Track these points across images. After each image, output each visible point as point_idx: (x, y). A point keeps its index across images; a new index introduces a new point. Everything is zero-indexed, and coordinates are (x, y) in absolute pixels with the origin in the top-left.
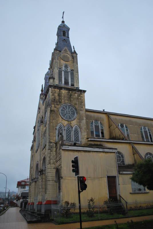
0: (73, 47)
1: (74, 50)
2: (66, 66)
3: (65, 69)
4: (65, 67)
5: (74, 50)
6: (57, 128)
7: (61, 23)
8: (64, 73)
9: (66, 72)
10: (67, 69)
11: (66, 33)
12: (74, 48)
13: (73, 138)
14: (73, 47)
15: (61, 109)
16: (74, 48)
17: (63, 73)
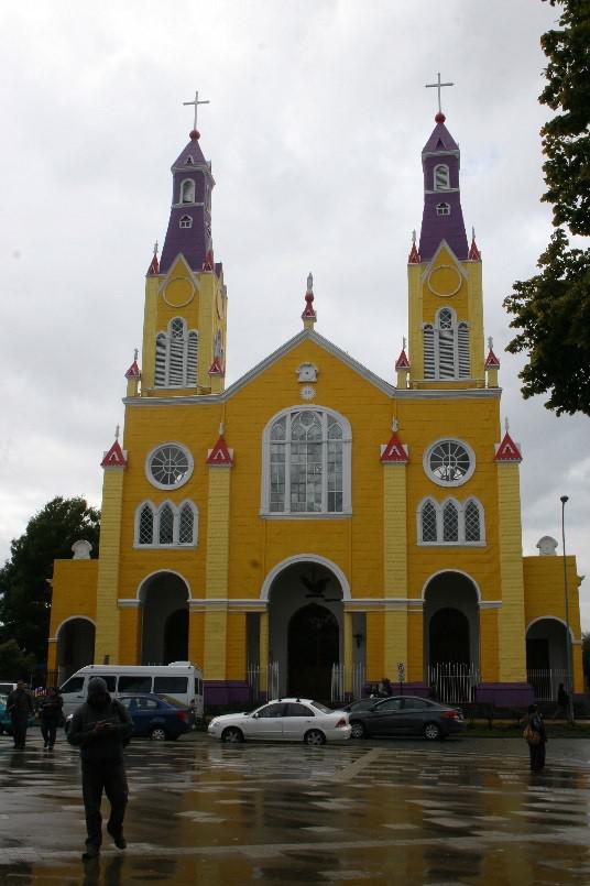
4: (441, 316)
6: (420, 508)
13: (461, 534)
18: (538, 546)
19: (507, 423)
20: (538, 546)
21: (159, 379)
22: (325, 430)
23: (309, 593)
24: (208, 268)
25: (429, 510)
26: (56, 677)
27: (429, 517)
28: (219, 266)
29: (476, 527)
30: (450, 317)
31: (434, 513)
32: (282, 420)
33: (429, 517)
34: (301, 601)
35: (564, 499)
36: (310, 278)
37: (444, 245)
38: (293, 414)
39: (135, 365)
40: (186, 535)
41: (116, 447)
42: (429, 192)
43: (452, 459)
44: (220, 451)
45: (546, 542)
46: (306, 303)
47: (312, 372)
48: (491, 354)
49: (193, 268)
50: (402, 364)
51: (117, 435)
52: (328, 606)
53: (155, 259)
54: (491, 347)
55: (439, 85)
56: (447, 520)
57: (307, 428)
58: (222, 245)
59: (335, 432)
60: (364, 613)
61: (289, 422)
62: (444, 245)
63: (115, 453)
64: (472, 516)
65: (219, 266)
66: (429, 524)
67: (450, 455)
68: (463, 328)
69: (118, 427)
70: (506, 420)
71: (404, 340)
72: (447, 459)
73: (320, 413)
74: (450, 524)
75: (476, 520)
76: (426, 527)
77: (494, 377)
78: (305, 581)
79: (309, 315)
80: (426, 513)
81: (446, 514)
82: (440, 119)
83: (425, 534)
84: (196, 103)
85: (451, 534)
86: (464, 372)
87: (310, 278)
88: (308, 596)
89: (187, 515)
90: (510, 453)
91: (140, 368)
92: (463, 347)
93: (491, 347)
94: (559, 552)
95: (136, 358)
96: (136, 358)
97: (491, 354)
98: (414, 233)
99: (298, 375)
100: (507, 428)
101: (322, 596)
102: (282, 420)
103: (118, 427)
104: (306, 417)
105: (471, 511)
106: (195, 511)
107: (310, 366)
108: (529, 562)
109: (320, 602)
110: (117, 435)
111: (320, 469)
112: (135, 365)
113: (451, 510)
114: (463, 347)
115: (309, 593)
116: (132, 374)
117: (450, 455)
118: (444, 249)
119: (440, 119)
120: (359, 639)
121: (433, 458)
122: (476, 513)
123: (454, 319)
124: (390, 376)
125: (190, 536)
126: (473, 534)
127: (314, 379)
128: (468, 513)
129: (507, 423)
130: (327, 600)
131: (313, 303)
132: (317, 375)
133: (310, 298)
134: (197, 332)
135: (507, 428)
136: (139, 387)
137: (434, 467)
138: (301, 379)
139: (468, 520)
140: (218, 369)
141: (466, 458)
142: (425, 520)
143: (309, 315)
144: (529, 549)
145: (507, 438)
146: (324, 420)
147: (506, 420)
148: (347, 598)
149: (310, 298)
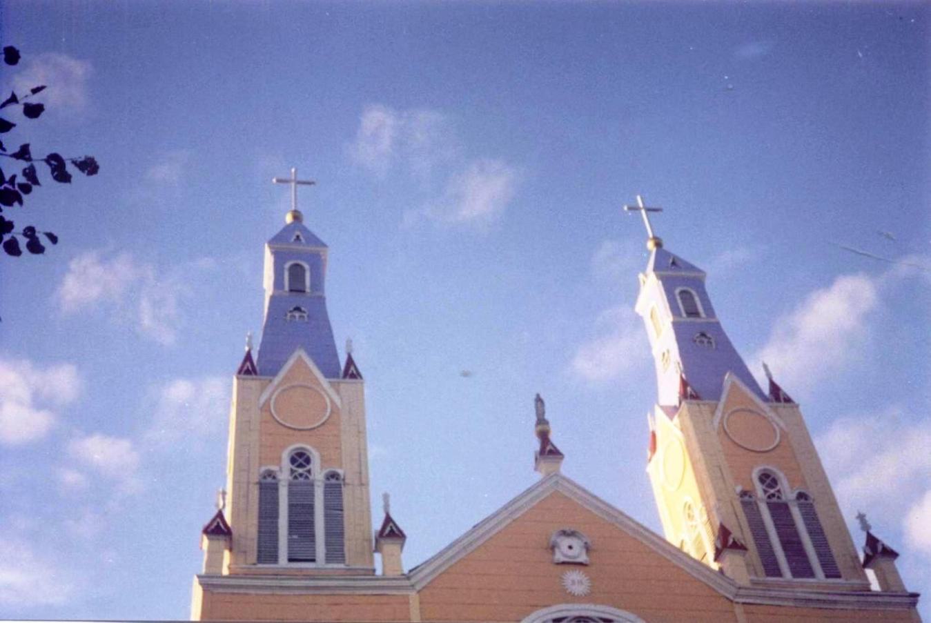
9: (780, 510)
21: (267, 552)
36: (539, 400)
42: (679, 319)
49: (326, 376)
50: (725, 542)
53: (248, 357)
54: (865, 526)
79: (548, 452)
87: (539, 400)
99: (553, 548)
107: (572, 534)
127: (583, 558)
132: (588, 549)
134: (340, 472)
138: (559, 557)
143: (548, 452)
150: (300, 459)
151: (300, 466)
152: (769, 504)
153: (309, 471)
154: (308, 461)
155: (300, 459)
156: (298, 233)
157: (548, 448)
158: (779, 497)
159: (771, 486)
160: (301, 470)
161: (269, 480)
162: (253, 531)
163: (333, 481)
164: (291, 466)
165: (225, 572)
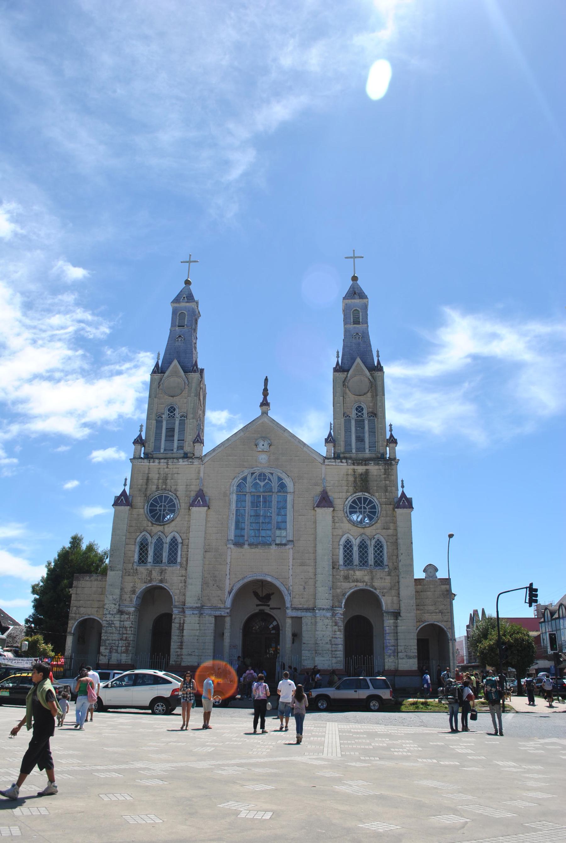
0: (378, 352)
1: (378, 360)
2: (359, 409)
3: (357, 414)
4: (357, 409)
5: (378, 360)
6: (342, 541)
7: (351, 282)
8: (356, 424)
9: (360, 423)
10: (363, 414)
11: (361, 314)
12: (378, 356)
14: (378, 352)
15: (349, 505)
16: (378, 356)
17: (353, 423)
18: (424, 571)
19: (402, 484)
20: (424, 571)
22: (275, 485)
23: (261, 603)
24: (195, 372)
25: (348, 544)
26: (71, 661)
27: (348, 549)
28: (202, 371)
29: (381, 557)
30: (362, 409)
31: (351, 546)
32: (245, 479)
33: (348, 549)
34: (252, 607)
35: (451, 536)
36: (266, 380)
37: (358, 360)
38: (252, 474)
39: (140, 436)
40: (172, 560)
41: (124, 491)
43: (365, 508)
44: (199, 498)
45: (431, 569)
46: (262, 397)
47: (266, 444)
48: (392, 436)
50: (329, 440)
51: (125, 485)
52: (274, 613)
53: (157, 364)
54: (391, 430)
55: (354, 257)
56: (360, 552)
57: (262, 484)
58: (204, 358)
59: (282, 486)
60: (301, 618)
61: (249, 479)
62: (358, 360)
63: (122, 498)
64: (378, 549)
65: (202, 371)
66: (348, 554)
67: (363, 505)
68: (372, 418)
69: (126, 479)
70: (402, 481)
71: (331, 424)
72: (360, 508)
73: (272, 474)
74: (363, 554)
75: (381, 552)
76: (345, 556)
77: (393, 451)
78: (256, 594)
79: (265, 404)
80: (345, 546)
81: (360, 547)
82: (355, 279)
83: (345, 561)
84: (189, 262)
85: (363, 561)
86: (373, 446)
87: (266, 380)
88: (257, 605)
89: (174, 543)
90: (406, 503)
91: (144, 438)
92: (373, 432)
93: (391, 430)
94: (441, 574)
95: (141, 431)
96: (141, 431)
97: (392, 436)
98: (338, 352)
100: (403, 487)
101: (269, 606)
102: (245, 479)
103: (126, 479)
104: (262, 477)
105: (379, 546)
106: (180, 540)
108: (418, 581)
109: (267, 610)
110: (125, 485)
111: (271, 513)
112: (140, 436)
113: (363, 544)
114: (373, 432)
115: (261, 603)
116: (139, 441)
117: (363, 505)
118: (358, 363)
119: (355, 279)
120: (296, 636)
121: (351, 507)
122: (381, 547)
123: (365, 412)
124: (323, 450)
125: (176, 559)
126: (379, 563)
128: (376, 547)
129: (402, 484)
130: (271, 609)
131: (268, 398)
132: (270, 445)
133: (265, 392)
135: (403, 487)
136: (143, 451)
137: (351, 513)
139: (376, 551)
140: (199, 440)
141: (374, 507)
142: (345, 551)
143: (265, 404)
144: (419, 574)
145: (403, 493)
146: (274, 479)
147: (402, 481)
148: (288, 605)
149: (265, 392)
150: (172, 410)
151: (172, 412)
152: (356, 421)
153: (174, 414)
154: (174, 410)
155: (172, 410)
156: (185, 296)
157: (265, 402)
158: (362, 417)
159: (360, 412)
160: (172, 414)
161: (160, 419)
162: (152, 439)
163: (183, 418)
164: (168, 412)
165: (142, 456)
